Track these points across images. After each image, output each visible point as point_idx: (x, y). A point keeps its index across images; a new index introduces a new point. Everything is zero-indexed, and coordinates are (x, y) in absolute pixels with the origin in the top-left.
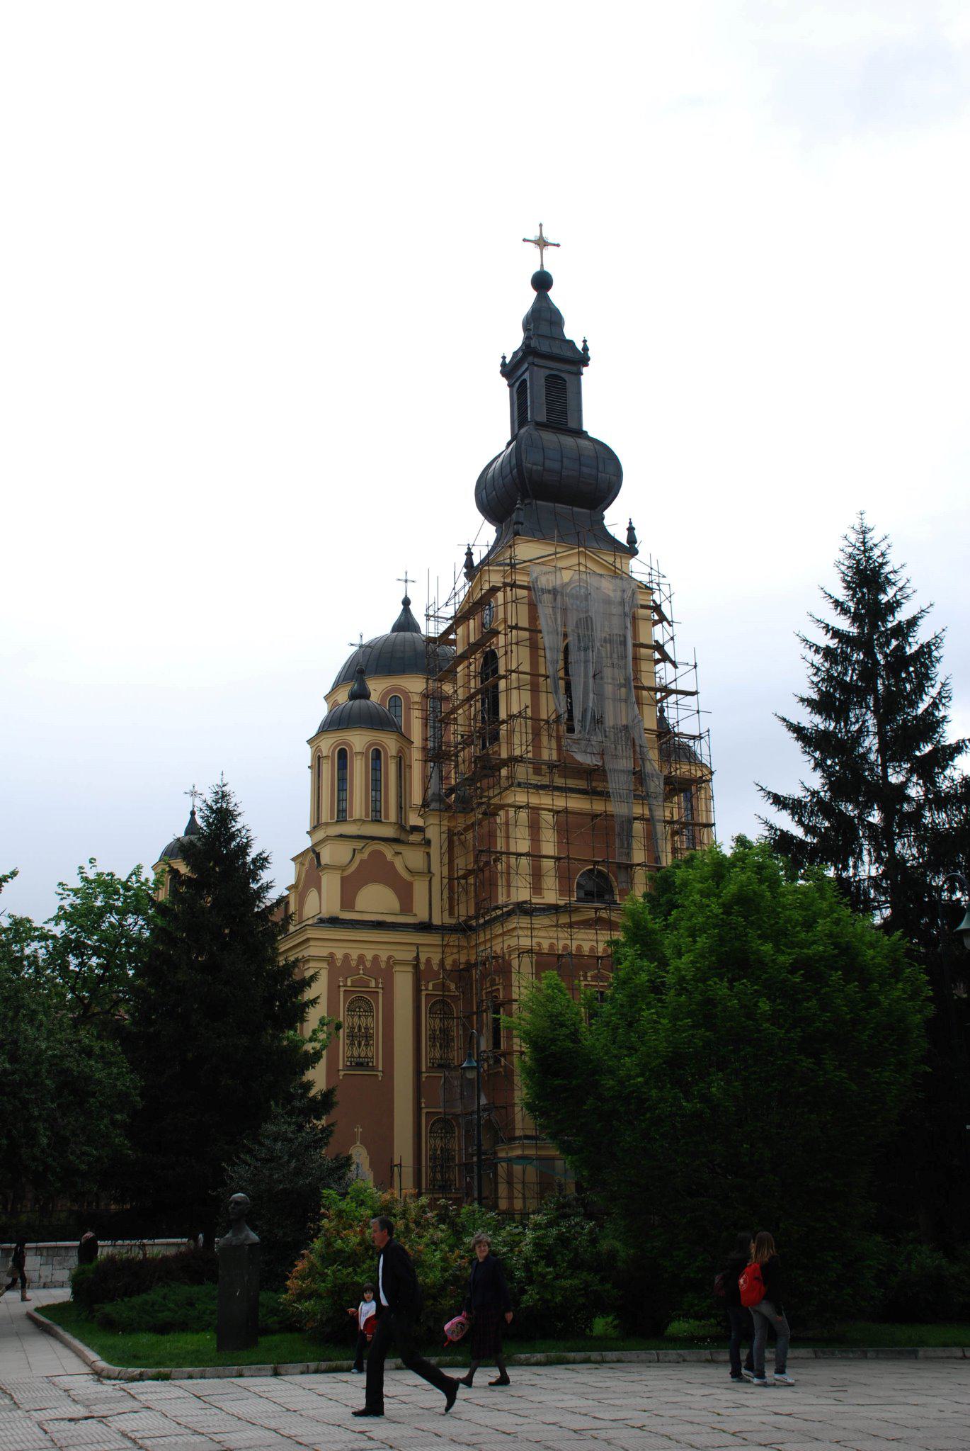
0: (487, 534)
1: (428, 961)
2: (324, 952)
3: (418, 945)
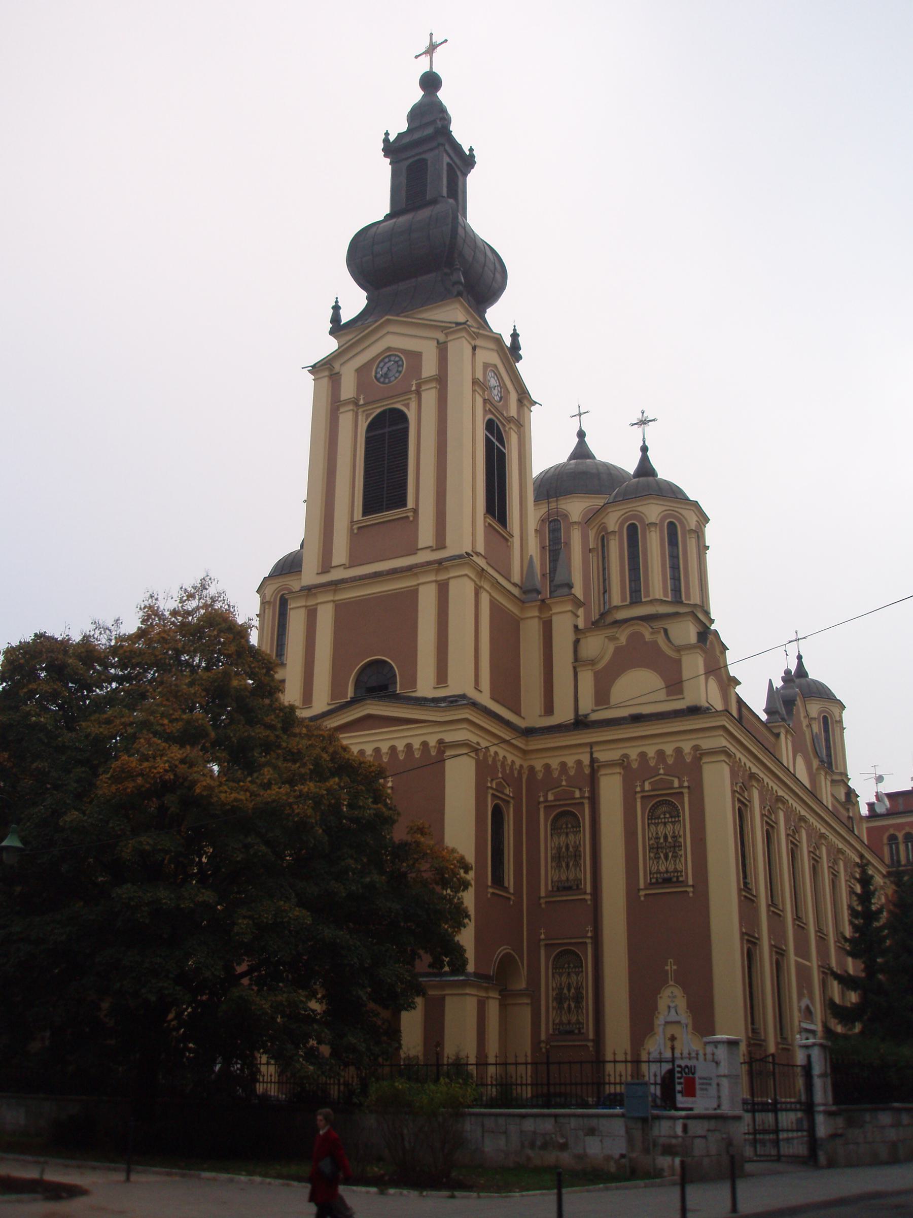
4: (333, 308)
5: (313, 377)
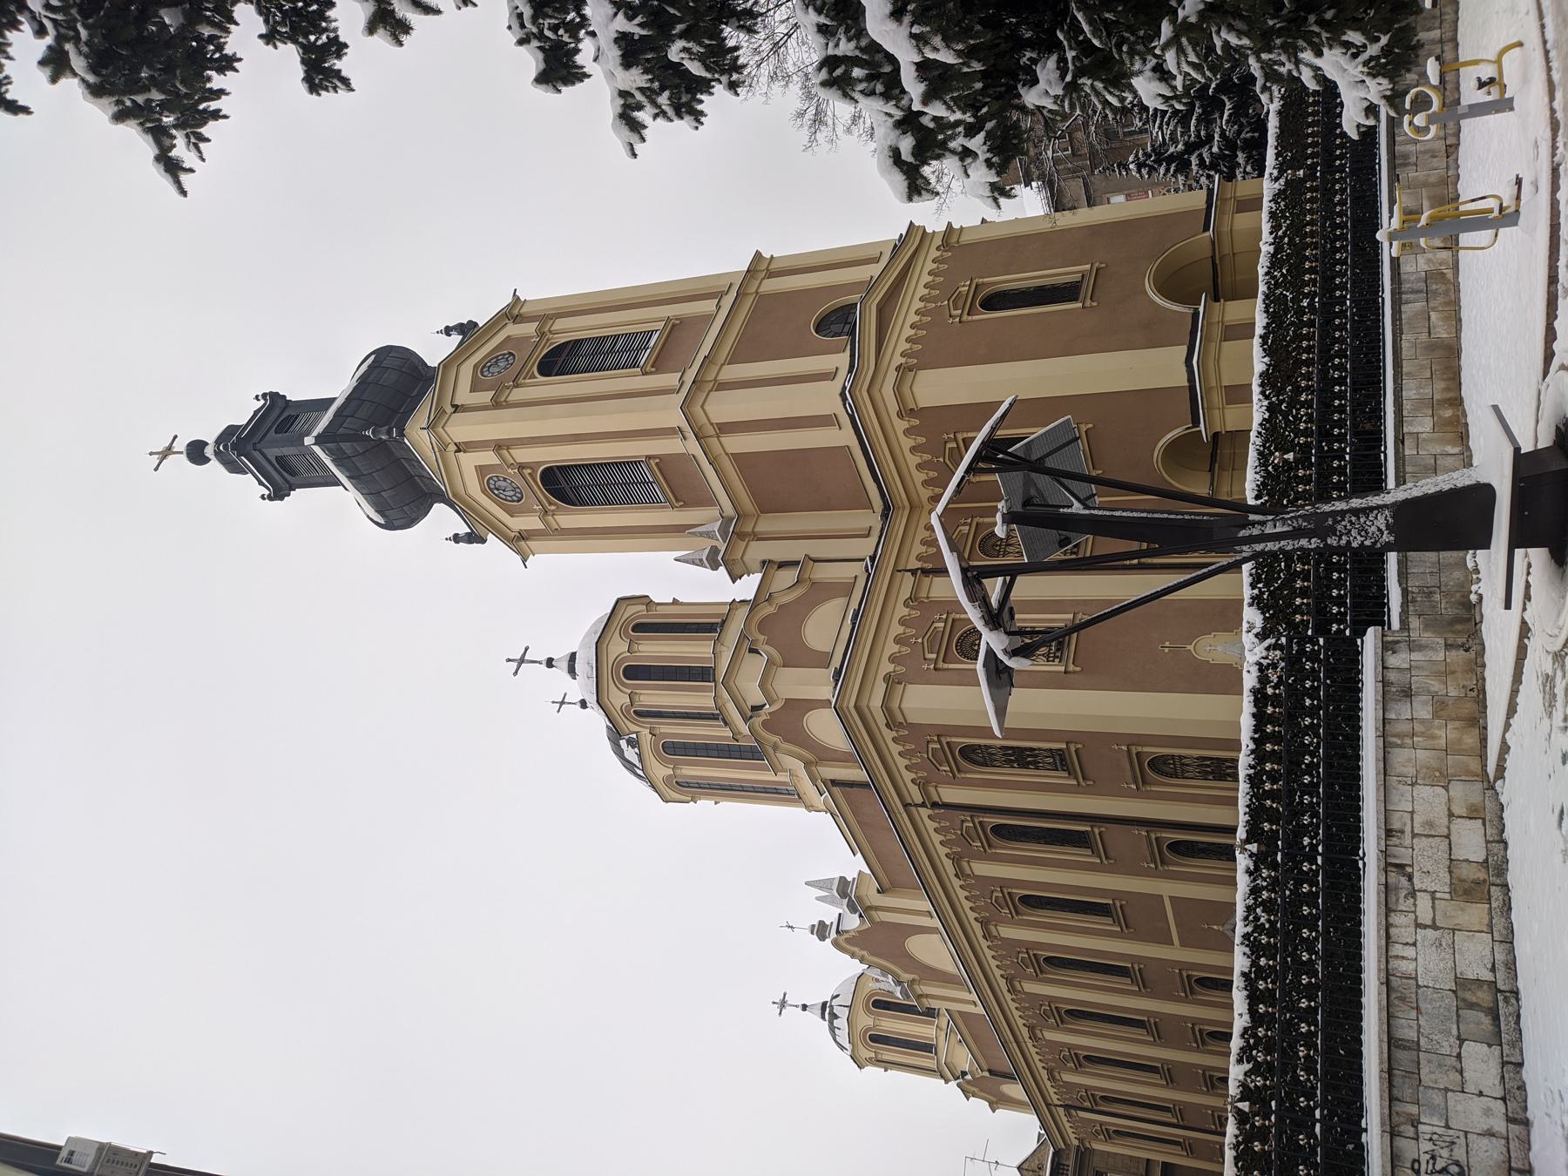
0: (442, 520)
1: (919, 558)
2: (880, 688)
3: (896, 570)
4: (457, 542)
5: (531, 556)
